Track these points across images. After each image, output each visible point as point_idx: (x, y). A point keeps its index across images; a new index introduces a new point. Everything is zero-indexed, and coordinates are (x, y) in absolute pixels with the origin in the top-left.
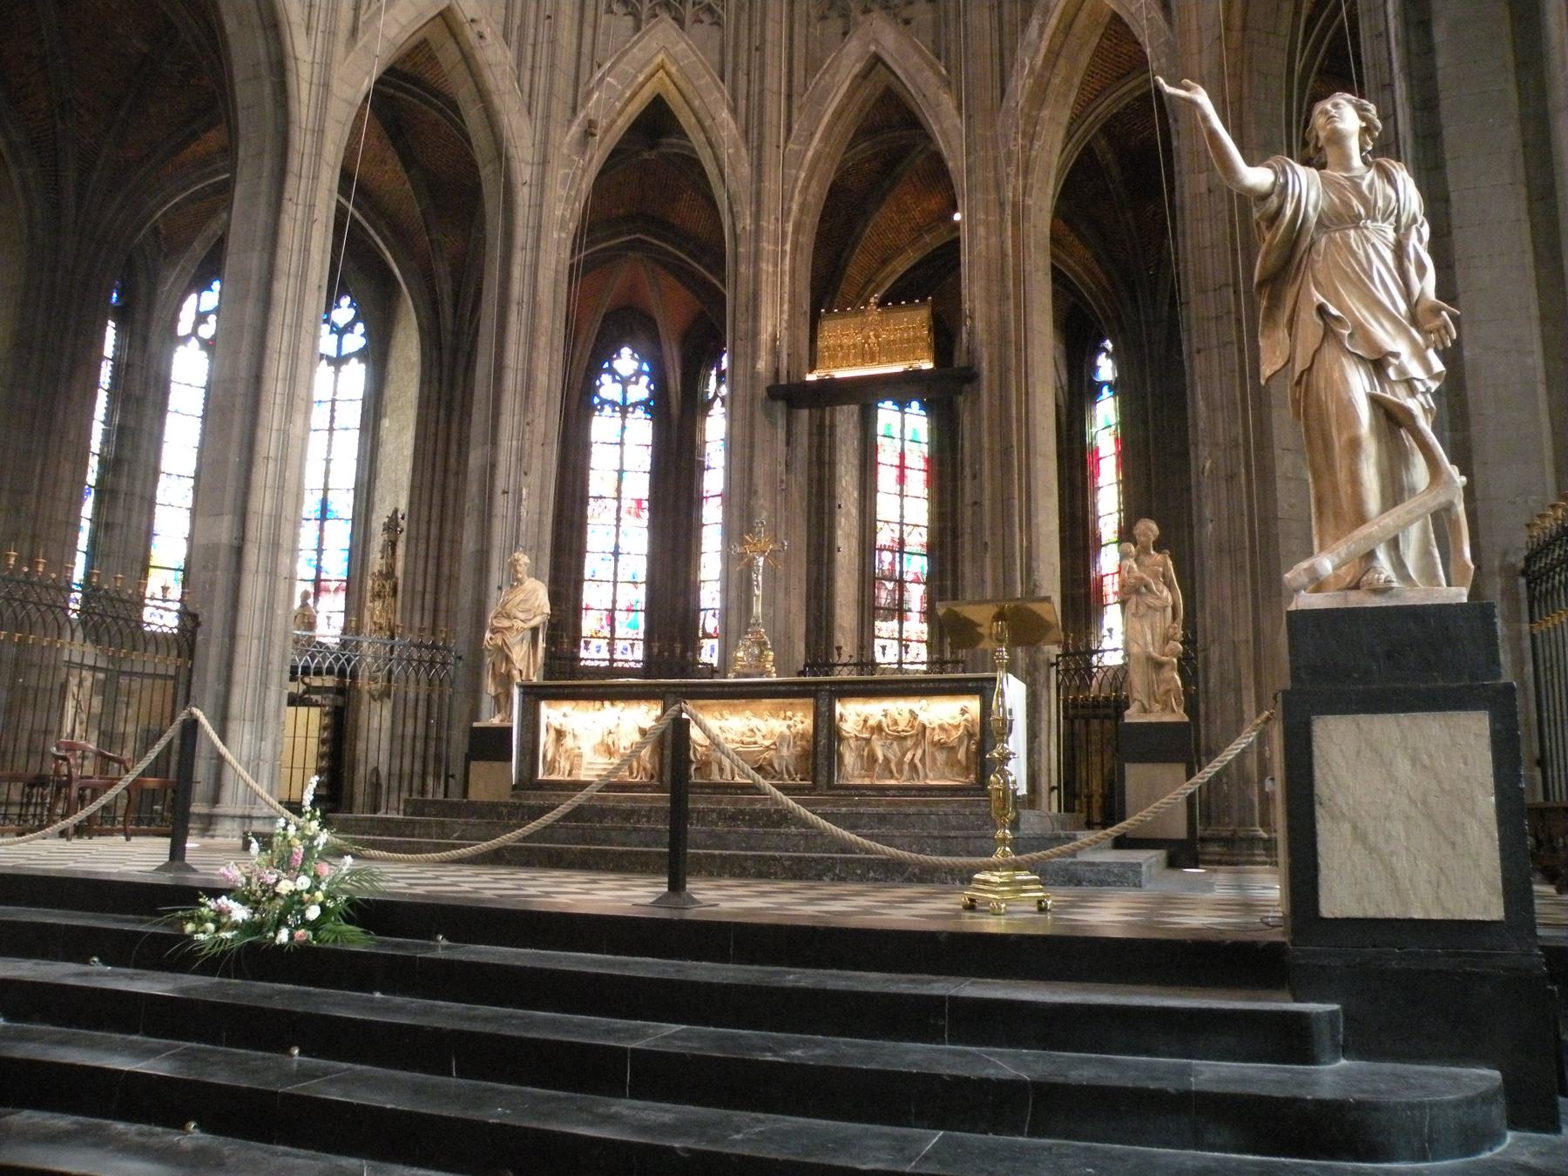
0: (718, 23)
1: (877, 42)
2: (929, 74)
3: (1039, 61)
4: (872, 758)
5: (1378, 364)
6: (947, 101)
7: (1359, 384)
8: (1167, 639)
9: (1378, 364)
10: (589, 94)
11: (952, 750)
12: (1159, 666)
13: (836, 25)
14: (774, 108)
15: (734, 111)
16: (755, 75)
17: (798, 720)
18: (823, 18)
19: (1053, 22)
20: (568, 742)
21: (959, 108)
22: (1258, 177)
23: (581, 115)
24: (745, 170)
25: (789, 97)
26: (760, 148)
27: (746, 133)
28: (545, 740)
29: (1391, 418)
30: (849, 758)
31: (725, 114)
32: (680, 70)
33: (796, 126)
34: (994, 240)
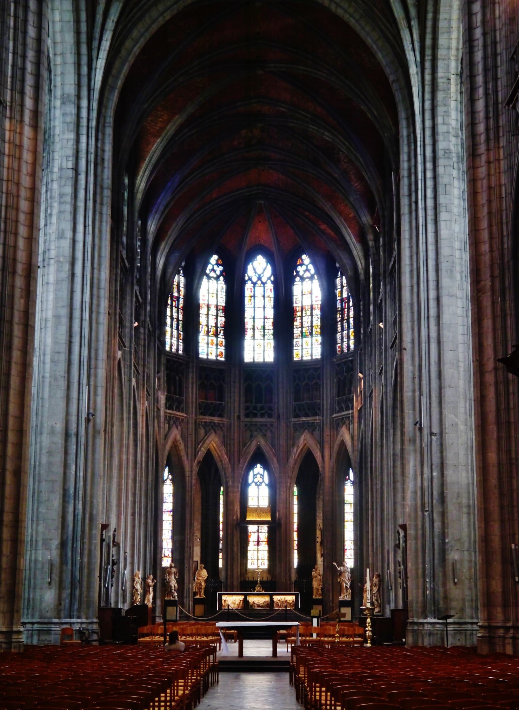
0: (222, 430)
1: (259, 442)
2: (271, 452)
3: (296, 457)
4: (278, 605)
5: (346, 583)
6: (275, 460)
7: (345, 585)
8: (320, 585)
9: (346, 583)
10: (198, 453)
11: (291, 604)
12: (318, 589)
13: (248, 434)
14: (236, 455)
15: (227, 455)
16: (232, 446)
17: (267, 599)
18: (246, 431)
19: (299, 450)
20: (227, 602)
21: (278, 461)
22: (339, 569)
23: (197, 458)
24: (230, 470)
25: (239, 452)
26: (234, 465)
27: (230, 460)
28: (223, 602)
29: (346, 587)
30: (275, 605)
31: (226, 456)
32: (216, 445)
33: (241, 460)
34: (285, 495)
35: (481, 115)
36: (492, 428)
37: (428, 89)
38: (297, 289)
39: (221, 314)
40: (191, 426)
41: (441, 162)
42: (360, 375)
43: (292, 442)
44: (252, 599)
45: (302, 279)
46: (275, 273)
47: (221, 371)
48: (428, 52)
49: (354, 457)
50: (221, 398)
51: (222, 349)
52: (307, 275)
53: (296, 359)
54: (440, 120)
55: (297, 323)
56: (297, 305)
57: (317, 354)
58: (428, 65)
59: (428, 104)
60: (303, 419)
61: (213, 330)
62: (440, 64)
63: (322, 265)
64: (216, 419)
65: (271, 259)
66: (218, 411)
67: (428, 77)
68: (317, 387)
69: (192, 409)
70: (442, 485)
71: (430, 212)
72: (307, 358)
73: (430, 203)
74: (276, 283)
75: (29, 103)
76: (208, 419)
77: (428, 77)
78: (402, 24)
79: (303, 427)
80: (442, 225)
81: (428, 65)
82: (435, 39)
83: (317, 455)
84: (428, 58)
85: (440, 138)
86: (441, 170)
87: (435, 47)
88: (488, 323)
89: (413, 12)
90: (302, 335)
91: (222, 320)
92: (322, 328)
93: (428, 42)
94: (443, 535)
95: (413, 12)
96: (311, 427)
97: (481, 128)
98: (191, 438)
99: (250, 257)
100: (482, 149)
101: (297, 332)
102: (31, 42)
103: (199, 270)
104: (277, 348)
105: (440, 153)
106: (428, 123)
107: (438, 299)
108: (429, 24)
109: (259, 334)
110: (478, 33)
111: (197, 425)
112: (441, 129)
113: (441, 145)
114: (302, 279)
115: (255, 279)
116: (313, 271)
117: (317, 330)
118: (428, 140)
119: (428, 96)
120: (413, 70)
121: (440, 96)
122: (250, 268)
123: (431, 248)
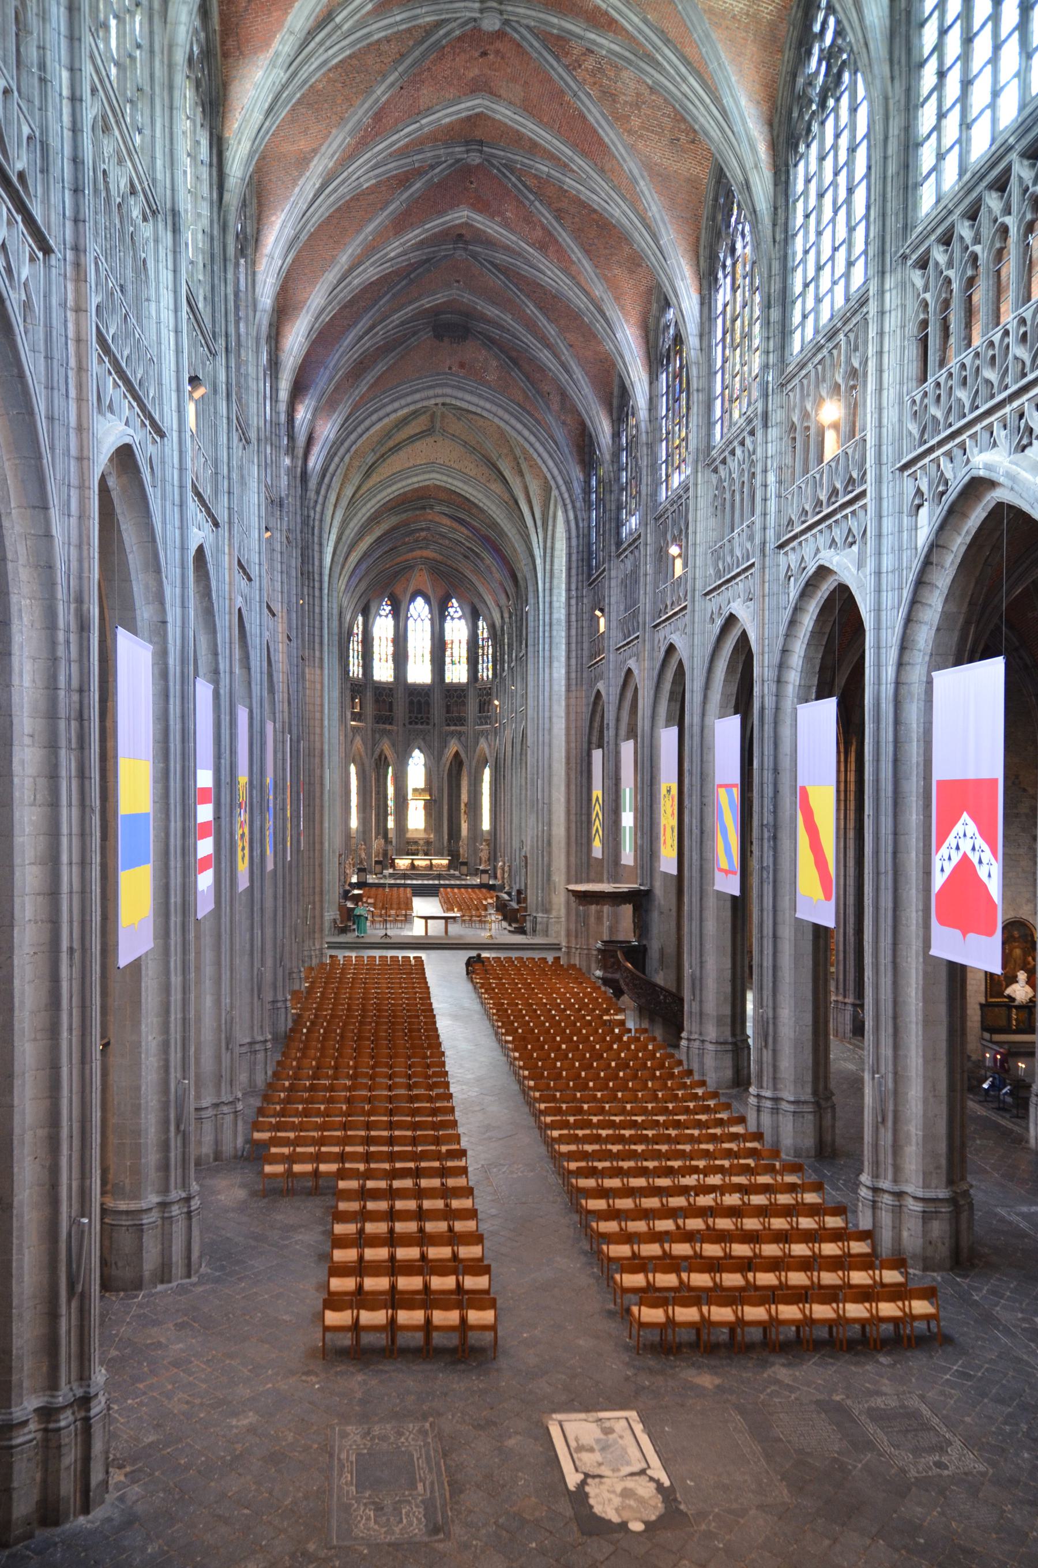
35: (573, 668)
36: (573, 845)
37: (548, 575)
38: (448, 625)
39: (390, 644)
40: (369, 732)
41: (555, 627)
42: (496, 702)
43: (444, 744)
44: (416, 863)
45: (453, 618)
46: (431, 611)
47: (391, 690)
48: (548, 551)
49: (491, 760)
50: (391, 710)
51: (392, 672)
52: (456, 615)
53: (448, 680)
54: (555, 598)
55: (448, 653)
56: (448, 637)
57: (464, 679)
58: (548, 559)
59: (547, 585)
60: (453, 728)
61: (384, 658)
62: (556, 560)
63: (468, 610)
64: (388, 727)
65: (428, 601)
66: (389, 720)
67: (548, 567)
68: (464, 704)
69: (370, 719)
70: (550, 835)
71: (547, 660)
72: (455, 681)
73: (547, 654)
74: (432, 620)
75: (317, 653)
76: (382, 726)
77: (548, 567)
78: (532, 530)
79: (453, 734)
80: (554, 670)
81: (548, 559)
82: (553, 543)
83: (463, 755)
84: (548, 555)
85: (555, 611)
86: (554, 633)
87: (553, 548)
88: (573, 787)
89: (539, 523)
90: (453, 663)
91: (391, 649)
92: (468, 659)
93: (549, 544)
94: (549, 865)
95: (539, 523)
96: (460, 734)
97: (573, 675)
98: (370, 743)
99: (412, 599)
100: (573, 688)
101: (448, 660)
102: (317, 617)
103: (373, 610)
104: (433, 671)
105: (554, 622)
106: (547, 599)
107: (550, 718)
108: (550, 533)
109: (419, 659)
110: (573, 618)
111: (374, 731)
112: (555, 605)
113: (555, 616)
114: (453, 618)
115: (415, 616)
116: (460, 613)
117: (464, 660)
118: (547, 611)
119: (547, 580)
120: (539, 561)
121: (555, 582)
122: (412, 607)
123: (547, 684)
